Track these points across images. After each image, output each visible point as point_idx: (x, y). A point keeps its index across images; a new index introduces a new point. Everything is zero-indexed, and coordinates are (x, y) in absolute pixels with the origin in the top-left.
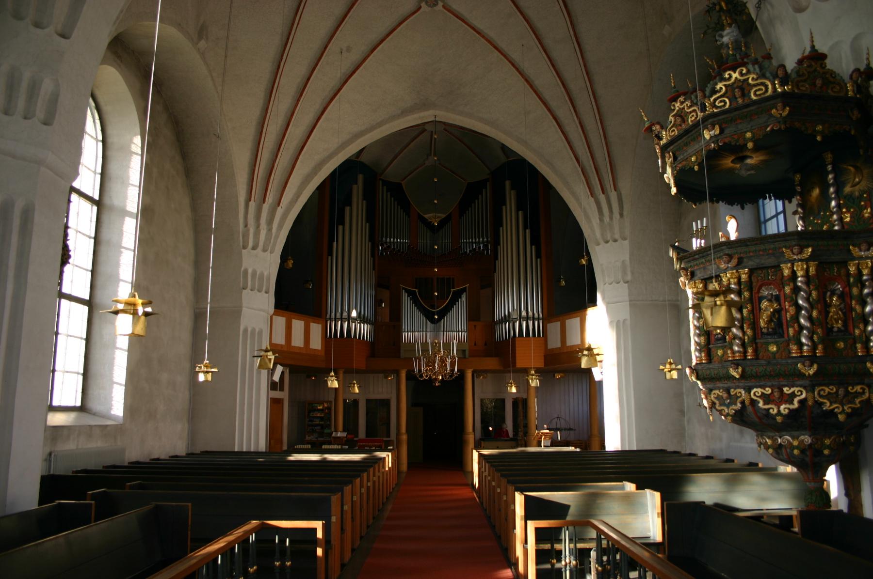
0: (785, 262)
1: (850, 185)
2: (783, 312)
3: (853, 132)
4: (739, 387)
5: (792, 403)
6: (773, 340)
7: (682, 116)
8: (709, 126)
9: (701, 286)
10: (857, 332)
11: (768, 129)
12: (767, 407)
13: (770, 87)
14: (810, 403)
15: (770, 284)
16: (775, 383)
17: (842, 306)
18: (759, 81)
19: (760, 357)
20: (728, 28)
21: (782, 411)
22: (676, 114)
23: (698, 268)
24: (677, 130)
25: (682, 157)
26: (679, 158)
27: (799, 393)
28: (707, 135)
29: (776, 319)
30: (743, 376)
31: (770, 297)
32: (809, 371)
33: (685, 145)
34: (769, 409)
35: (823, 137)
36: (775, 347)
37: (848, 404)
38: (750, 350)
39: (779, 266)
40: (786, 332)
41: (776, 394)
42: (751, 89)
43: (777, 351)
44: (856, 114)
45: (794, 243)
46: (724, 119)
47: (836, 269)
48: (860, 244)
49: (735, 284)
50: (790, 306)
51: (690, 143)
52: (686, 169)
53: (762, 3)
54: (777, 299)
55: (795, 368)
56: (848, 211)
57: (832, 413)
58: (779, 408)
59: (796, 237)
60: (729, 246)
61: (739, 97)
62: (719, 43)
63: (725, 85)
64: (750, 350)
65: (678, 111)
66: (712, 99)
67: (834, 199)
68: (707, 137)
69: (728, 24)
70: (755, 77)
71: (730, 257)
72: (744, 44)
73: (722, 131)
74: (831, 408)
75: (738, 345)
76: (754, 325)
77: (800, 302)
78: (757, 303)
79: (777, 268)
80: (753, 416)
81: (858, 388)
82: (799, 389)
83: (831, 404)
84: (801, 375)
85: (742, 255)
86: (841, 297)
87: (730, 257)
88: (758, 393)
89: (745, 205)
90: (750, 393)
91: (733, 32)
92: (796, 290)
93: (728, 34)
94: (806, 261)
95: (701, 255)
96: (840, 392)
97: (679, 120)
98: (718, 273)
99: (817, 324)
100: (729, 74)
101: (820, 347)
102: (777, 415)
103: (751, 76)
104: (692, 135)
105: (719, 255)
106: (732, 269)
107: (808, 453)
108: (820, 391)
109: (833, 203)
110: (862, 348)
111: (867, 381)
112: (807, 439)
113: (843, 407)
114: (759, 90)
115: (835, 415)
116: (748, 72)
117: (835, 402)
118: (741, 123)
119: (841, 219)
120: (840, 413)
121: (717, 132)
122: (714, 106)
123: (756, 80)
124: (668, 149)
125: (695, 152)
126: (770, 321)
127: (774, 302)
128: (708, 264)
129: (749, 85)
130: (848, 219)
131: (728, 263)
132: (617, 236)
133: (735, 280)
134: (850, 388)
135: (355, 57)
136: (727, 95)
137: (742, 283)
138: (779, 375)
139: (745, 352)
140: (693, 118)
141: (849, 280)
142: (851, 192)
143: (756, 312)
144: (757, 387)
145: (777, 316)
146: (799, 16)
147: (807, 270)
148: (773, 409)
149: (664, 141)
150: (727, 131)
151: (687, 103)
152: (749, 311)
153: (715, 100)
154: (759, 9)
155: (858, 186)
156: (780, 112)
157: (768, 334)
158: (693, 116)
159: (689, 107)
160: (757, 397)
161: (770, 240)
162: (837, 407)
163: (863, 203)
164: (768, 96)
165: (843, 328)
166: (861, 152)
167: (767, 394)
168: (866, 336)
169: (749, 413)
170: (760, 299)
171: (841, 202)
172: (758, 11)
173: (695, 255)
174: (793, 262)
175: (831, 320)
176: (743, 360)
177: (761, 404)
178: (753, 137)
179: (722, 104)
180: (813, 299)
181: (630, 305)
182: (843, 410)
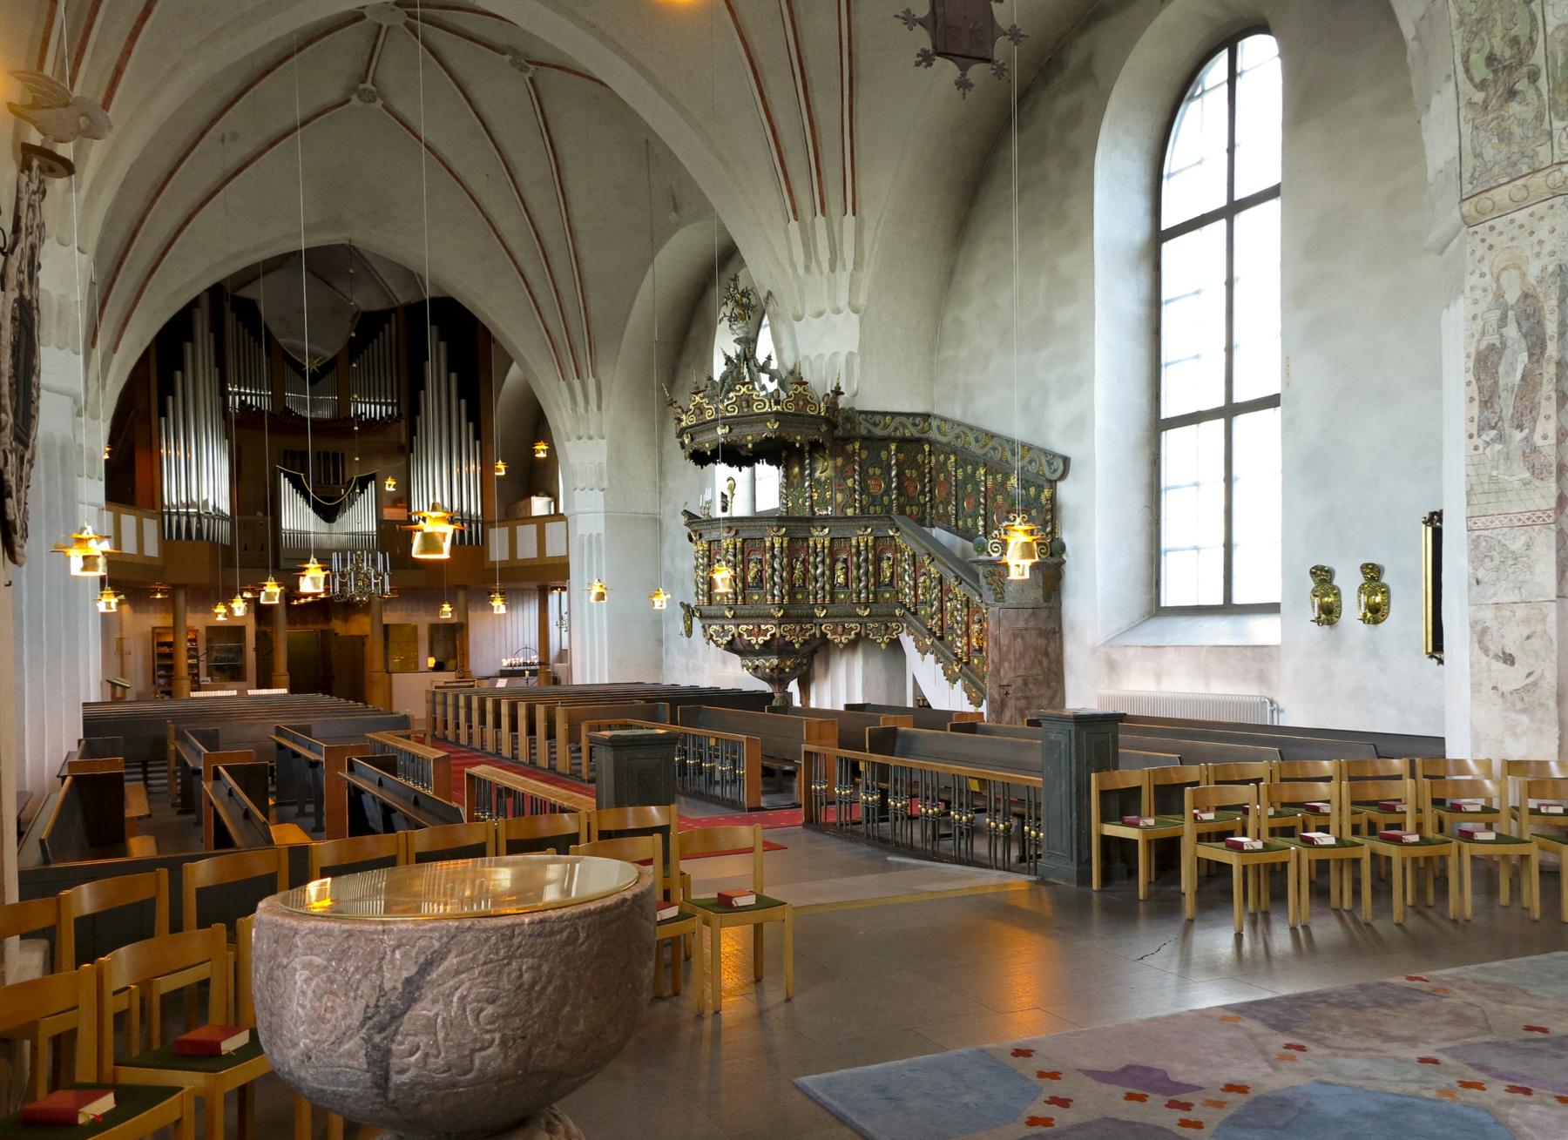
7: (700, 409)
9: (706, 546)
14: (778, 635)
16: (755, 622)
28: (720, 431)
30: (734, 617)
38: (740, 598)
41: (756, 630)
44: (824, 428)
56: (816, 492)
57: (791, 643)
64: (740, 598)
71: (730, 529)
73: (730, 431)
79: (762, 539)
81: (808, 626)
84: (772, 617)
86: (803, 562)
87: (730, 529)
92: (773, 557)
94: (782, 537)
109: (807, 484)
112: (775, 661)
115: (793, 644)
119: (811, 497)
132: (592, 433)
135: (244, 149)
136: (738, 403)
138: (758, 616)
139: (737, 599)
143: (745, 571)
146: (796, 324)
150: (734, 431)
156: (773, 426)
159: (708, 404)
177: (745, 637)
181: (606, 517)
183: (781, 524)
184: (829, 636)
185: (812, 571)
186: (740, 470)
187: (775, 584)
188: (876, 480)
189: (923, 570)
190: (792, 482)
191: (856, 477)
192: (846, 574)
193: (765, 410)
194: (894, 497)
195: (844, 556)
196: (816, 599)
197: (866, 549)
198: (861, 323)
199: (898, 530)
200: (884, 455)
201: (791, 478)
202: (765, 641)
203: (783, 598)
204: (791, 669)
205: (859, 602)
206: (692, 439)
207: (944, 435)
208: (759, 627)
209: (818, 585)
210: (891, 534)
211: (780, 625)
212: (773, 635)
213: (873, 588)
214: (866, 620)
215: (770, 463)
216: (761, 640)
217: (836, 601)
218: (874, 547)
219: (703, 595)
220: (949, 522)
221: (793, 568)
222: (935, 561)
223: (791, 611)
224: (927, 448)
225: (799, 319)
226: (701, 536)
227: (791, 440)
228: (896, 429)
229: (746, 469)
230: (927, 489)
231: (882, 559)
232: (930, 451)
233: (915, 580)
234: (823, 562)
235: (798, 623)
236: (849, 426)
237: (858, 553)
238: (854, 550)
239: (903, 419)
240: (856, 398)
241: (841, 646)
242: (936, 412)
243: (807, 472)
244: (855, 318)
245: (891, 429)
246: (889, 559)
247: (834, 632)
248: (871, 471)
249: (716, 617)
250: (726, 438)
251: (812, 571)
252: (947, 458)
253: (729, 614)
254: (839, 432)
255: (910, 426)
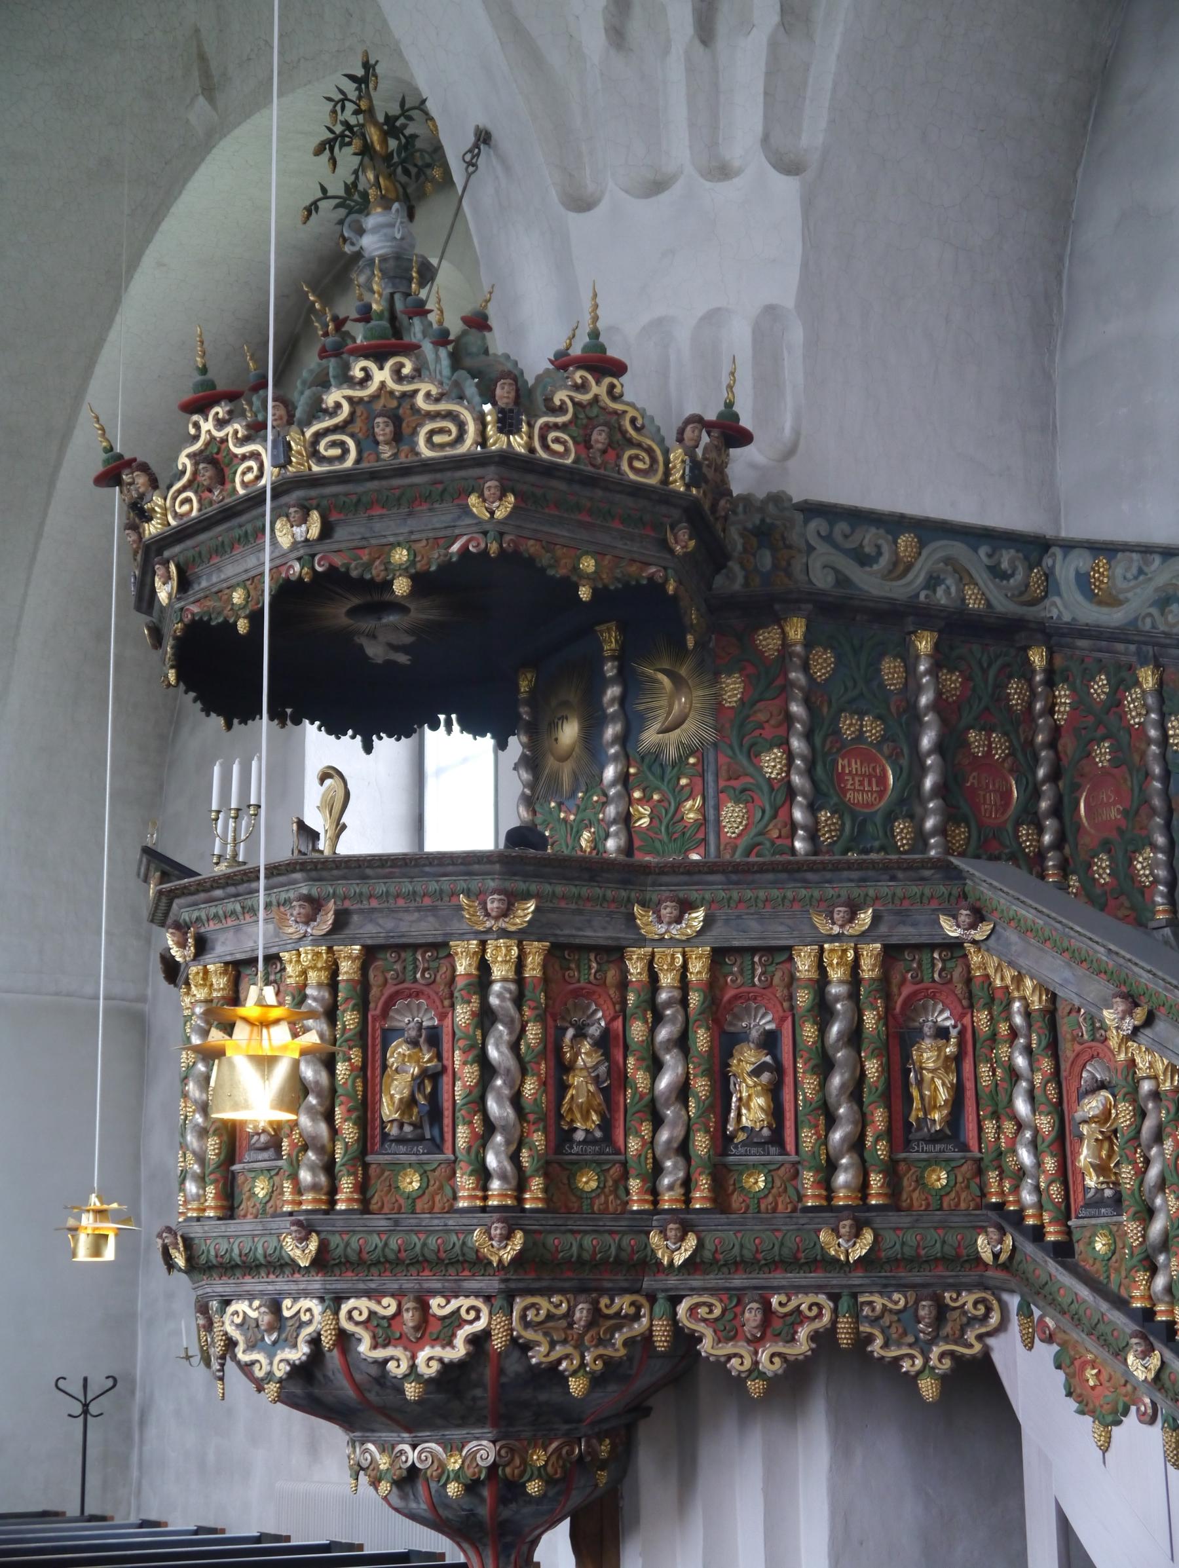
0: (462, 936)
1: (657, 726)
2: (446, 1079)
3: (671, 588)
4: (307, 1294)
5: (449, 1343)
6: (413, 1158)
8: (292, 510)
9: (220, 982)
10: (634, 1145)
11: (455, 548)
12: (380, 1354)
13: (471, 428)
14: (498, 1342)
15: (418, 995)
17: (603, 1069)
18: (443, 406)
19: (374, 1207)
20: (379, 210)
21: (422, 1369)
22: (201, 452)
23: (219, 926)
24: (200, 501)
25: (204, 584)
26: (196, 587)
27: (473, 1314)
28: (286, 535)
29: (425, 1097)
30: (321, 1262)
31: (413, 1033)
32: (502, 1253)
33: (217, 551)
34: (386, 1361)
35: (595, 592)
36: (417, 1177)
37: (596, 1346)
38: (346, 1184)
39: (445, 945)
40: (448, 1137)
41: (409, 1317)
42: (421, 425)
43: (423, 1190)
44: (683, 542)
45: (492, 884)
46: (336, 495)
47: (594, 965)
48: (659, 903)
49: (320, 985)
50: (465, 1063)
51: (232, 548)
52: (213, 623)
53: (482, 156)
54: (434, 1038)
55: (464, 1243)
56: (646, 799)
57: (552, 1375)
58: (413, 1357)
59: (497, 867)
60: (314, 874)
61: (387, 443)
62: (348, 249)
63: (349, 399)
64: (346, 1184)
65: (207, 444)
66: (309, 433)
67: (615, 758)
68: (285, 542)
69: (383, 197)
70: (434, 391)
71: (314, 905)
72: (418, 272)
73: (327, 530)
74: (554, 1356)
75: (312, 1168)
76: (365, 1112)
77: (493, 1053)
78: (378, 1048)
79: (440, 949)
80: (342, 1382)
82: (472, 1301)
83: (552, 1345)
84: (478, 1263)
85: (347, 904)
86: (604, 1043)
87: (314, 905)
88: (361, 1314)
89: (374, 737)
90: (336, 1312)
91: (392, 225)
92: (486, 1017)
93: (376, 229)
94: (521, 937)
95: (231, 890)
96: (577, 1315)
97: (208, 474)
98: (274, 950)
99: (531, 1117)
100: (364, 369)
101: (536, 1184)
102: (406, 1376)
103: (424, 387)
104: (240, 526)
105: (283, 896)
106: (316, 941)
107: (486, 1493)
108: (526, 1309)
109: (610, 773)
110: (641, 1191)
111: (647, 1283)
112: (484, 1451)
113: (583, 1357)
114: (441, 431)
115: (562, 1379)
116: (418, 374)
117: (565, 1342)
118: (381, 516)
119: (626, 819)
120: (574, 1373)
121: (315, 531)
122: (315, 454)
123: (437, 400)
124: (166, 554)
125: (245, 577)
126: (409, 1103)
127: (425, 1048)
128: (248, 919)
129: (415, 410)
130: (645, 822)
131: (307, 923)
133: (324, 976)
134: (604, 1301)
136: (350, 429)
137: (341, 986)
138: (420, 1262)
139: (333, 1190)
140: (249, 477)
141: (624, 1001)
142: (659, 745)
144: (358, 1294)
145: (429, 1090)
147: (520, 965)
148: (398, 1360)
149: (152, 529)
150: (340, 534)
151: (237, 426)
152: (353, 1068)
153: (318, 436)
154: (471, 169)
155: (678, 731)
157: (400, 1140)
158: (250, 469)
160: (357, 1323)
161: (427, 869)
162: (567, 1357)
163: (683, 781)
164: (463, 455)
165: (598, 1134)
166: (690, 641)
167: (384, 1318)
168: (654, 1158)
169: (330, 1374)
170: (388, 1036)
171: (632, 770)
172: (469, 175)
173: (212, 888)
174: (484, 937)
175: (570, 1110)
176: (326, 1212)
177: (364, 1348)
178: (413, 562)
179: (337, 452)
180: (528, 1046)
182: (583, 1365)
183: (521, 886)
184: (707, 1346)
185: (640, 1078)
186: (368, 748)
187: (490, 1127)
188: (867, 758)
189: (1093, 1071)
190: (555, 779)
191: (796, 744)
192: (774, 1092)
193: (463, 449)
194: (929, 824)
195: (767, 1022)
196: (654, 1192)
197: (854, 995)
198: (808, 204)
199: (979, 916)
200: (891, 671)
201: (551, 763)
202: (447, 1368)
203: (521, 1186)
204: (549, 1481)
205: (828, 1207)
206: (184, 584)
207: (1112, 601)
208: (424, 1307)
209: (664, 1135)
210: (951, 930)
211: (510, 1297)
212: (479, 1341)
213: (882, 1149)
214: (857, 1278)
215: (474, 727)
216: (430, 1361)
217: (736, 1200)
218: (884, 985)
219: (201, 1180)
220: (1139, 919)
221: (564, 1068)
222: (1161, 1026)
223: (552, 1241)
224: (1037, 658)
225: (582, 204)
226: (202, 946)
227: (562, 572)
228: (933, 582)
229: (385, 745)
230: (1044, 805)
231: (918, 1034)
232: (1050, 671)
233: (1060, 1112)
234: (682, 1042)
235: (581, 1290)
236: (766, 560)
237: (823, 1011)
238: (803, 998)
239: (957, 549)
240: (792, 463)
241: (755, 1387)
242: (1071, 529)
243: (610, 732)
244: (786, 188)
245: (917, 577)
246: (942, 1033)
247: (728, 1330)
248: (848, 726)
249: (249, 1266)
250: (307, 560)
251: (640, 1078)
252: (1123, 681)
253: (301, 1253)
254: (732, 581)
255: (982, 577)
